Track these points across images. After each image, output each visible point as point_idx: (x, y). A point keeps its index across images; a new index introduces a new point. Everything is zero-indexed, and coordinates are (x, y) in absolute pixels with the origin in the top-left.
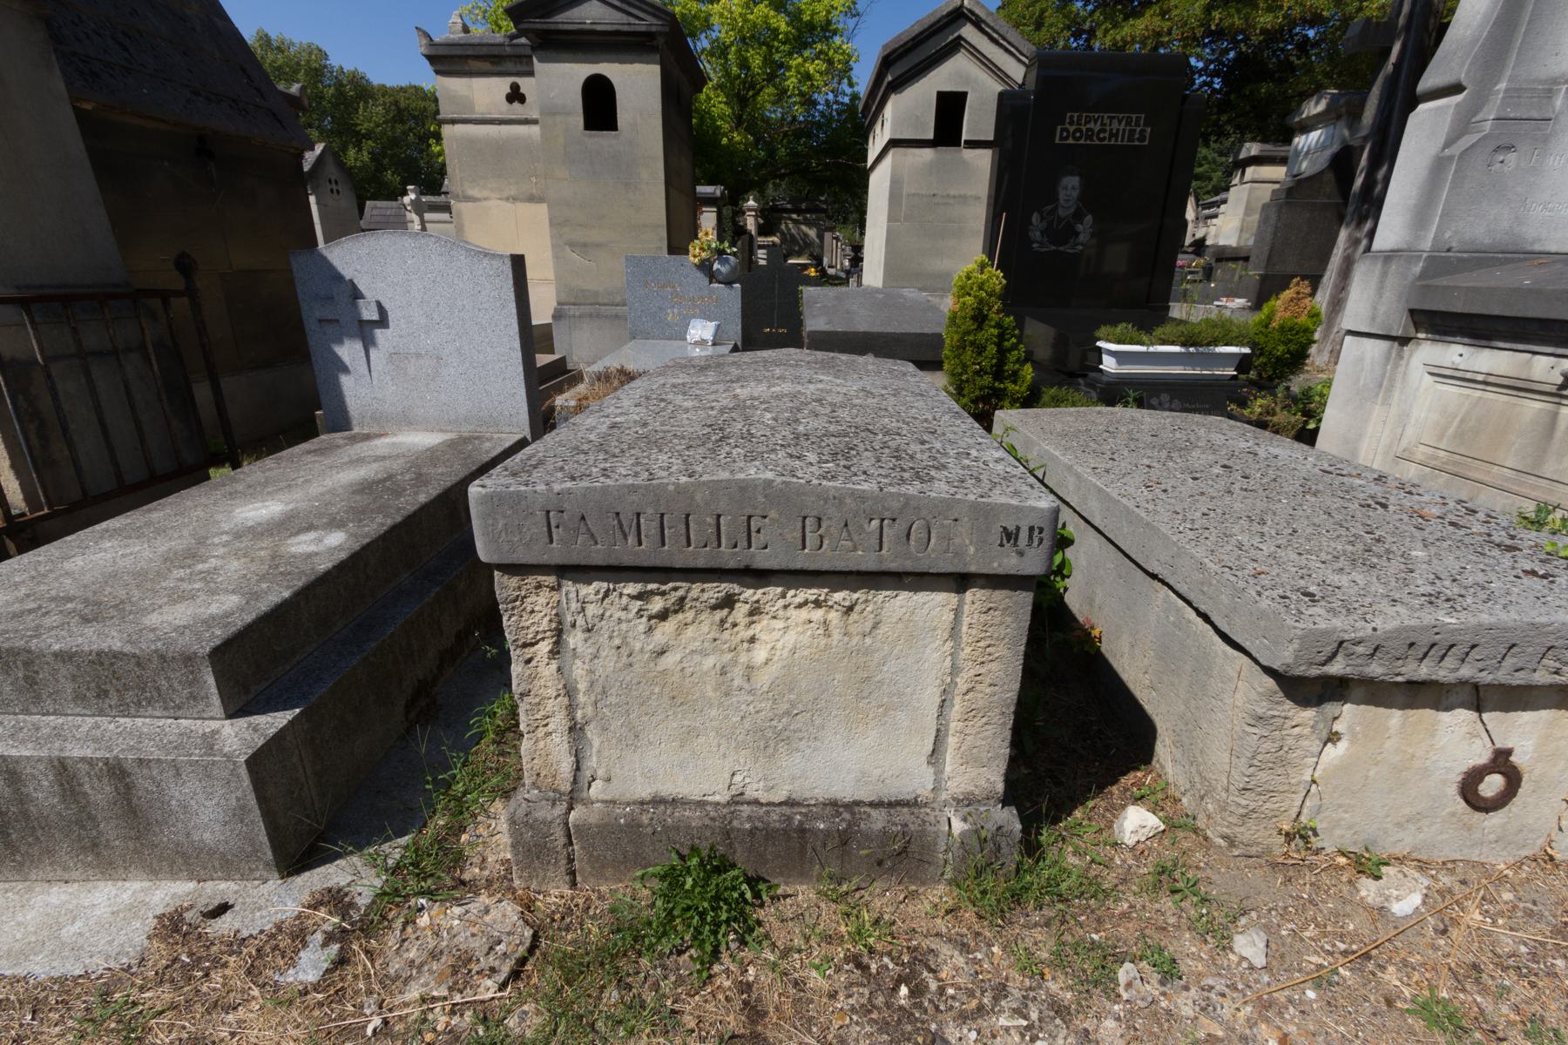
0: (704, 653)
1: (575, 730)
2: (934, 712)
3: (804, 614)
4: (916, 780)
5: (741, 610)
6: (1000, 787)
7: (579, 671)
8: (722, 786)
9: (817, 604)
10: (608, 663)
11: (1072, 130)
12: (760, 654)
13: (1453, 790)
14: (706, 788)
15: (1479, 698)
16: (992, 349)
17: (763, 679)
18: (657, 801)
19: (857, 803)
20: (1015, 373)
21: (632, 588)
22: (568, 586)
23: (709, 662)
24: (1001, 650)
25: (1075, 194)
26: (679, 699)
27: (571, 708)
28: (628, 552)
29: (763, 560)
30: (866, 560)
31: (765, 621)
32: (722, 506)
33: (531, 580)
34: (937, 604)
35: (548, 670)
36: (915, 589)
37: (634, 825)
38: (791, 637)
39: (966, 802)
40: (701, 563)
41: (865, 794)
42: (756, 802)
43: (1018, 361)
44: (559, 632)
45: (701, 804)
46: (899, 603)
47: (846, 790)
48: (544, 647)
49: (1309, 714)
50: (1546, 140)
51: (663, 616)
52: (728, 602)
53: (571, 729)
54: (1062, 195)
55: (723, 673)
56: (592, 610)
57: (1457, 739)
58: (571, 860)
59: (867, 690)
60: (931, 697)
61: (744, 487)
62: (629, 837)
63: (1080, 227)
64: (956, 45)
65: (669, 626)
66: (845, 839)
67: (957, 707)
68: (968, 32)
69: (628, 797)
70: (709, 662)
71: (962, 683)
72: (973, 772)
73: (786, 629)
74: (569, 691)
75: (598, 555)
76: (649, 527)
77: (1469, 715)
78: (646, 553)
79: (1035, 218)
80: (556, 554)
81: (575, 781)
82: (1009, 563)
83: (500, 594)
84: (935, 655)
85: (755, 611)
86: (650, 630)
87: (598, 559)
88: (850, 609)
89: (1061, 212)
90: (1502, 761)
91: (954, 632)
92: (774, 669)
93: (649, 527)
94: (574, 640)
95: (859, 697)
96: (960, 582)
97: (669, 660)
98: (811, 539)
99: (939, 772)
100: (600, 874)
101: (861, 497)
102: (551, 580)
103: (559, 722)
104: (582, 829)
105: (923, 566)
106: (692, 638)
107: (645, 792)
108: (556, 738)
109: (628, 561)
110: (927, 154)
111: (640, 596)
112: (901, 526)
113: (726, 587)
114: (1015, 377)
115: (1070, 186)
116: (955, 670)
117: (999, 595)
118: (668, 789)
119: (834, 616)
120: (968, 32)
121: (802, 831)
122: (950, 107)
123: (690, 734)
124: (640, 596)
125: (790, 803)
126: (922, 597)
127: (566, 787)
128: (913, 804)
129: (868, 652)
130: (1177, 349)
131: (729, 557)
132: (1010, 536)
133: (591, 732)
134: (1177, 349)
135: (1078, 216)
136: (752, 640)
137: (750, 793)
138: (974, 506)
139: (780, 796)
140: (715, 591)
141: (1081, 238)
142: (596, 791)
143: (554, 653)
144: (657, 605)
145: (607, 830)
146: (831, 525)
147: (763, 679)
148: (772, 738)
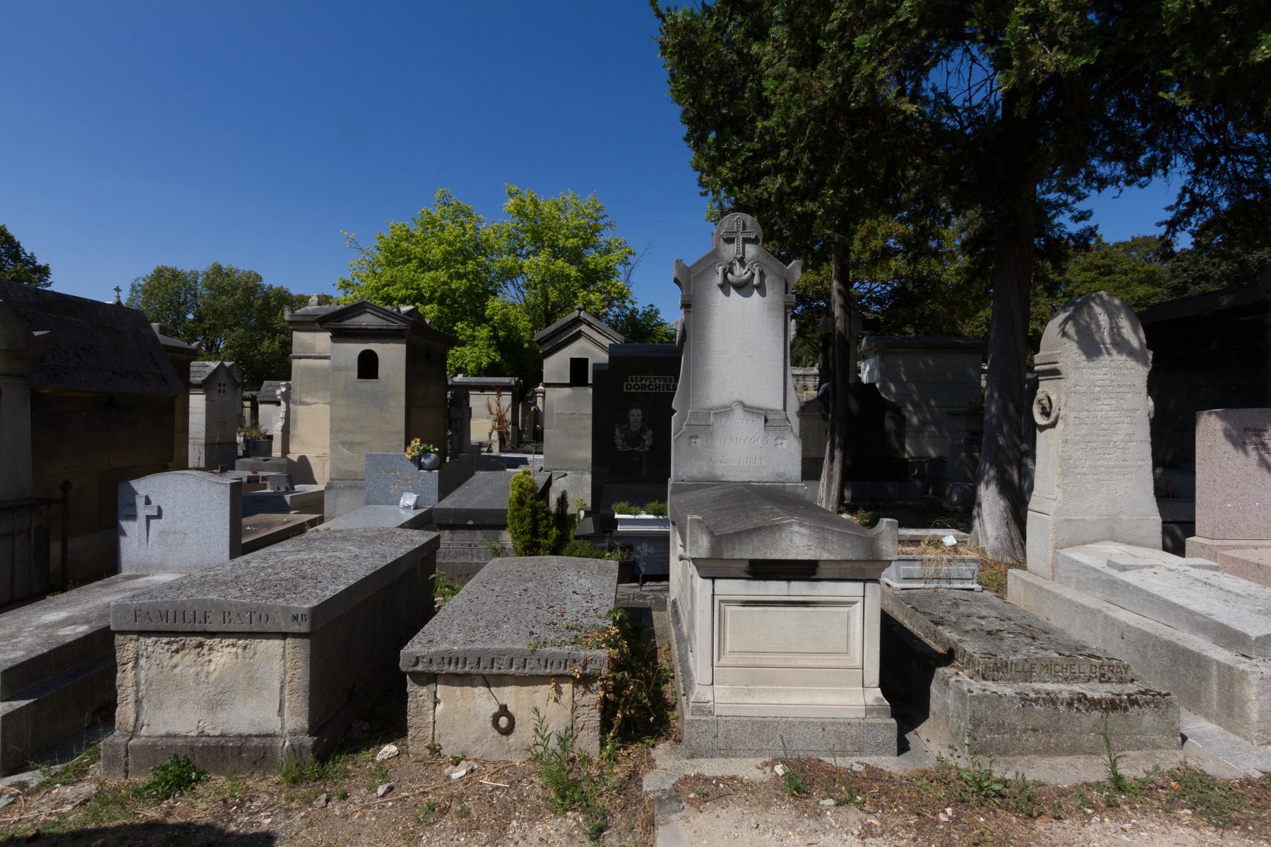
0: (190, 667)
1: (138, 702)
2: (278, 691)
3: (228, 650)
4: (274, 725)
5: (206, 648)
6: (307, 726)
7: (142, 675)
8: (194, 728)
9: (234, 645)
10: (154, 670)
11: (633, 384)
12: (212, 667)
13: (490, 725)
14: (188, 728)
15: (490, 681)
16: (528, 520)
17: (212, 677)
18: (168, 736)
19: (250, 736)
20: (546, 533)
21: (165, 640)
22: (142, 639)
23: (192, 670)
24: (300, 664)
25: (640, 418)
26: (179, 687)
27: (137, 691)
28: (163, 626)
29: (210, 628)
30: (246, 627)
31: (215, 653)
32: (196, 608)
33: (129, 637)
34: (276, 644)
35: (130, 675)
36: (268, 639)
37: (155, 745)
38: (224, 659)
39: (294, 733)
40: (188, 629)
41: (253, 731)
42: (209, 736)
43: (547, 525)
44: (137, 659)
45: (186, 737)
46: (263, 645)
47: (245, 729)
48: (131, 665)
49: (424, 690)
50: (711, 433)
51: (177, 651)
52: (201, 645)
53: (136, 701)
54: (632, 419)
55: (197, 674)
56: (150, 649)
57: (482, 701)
58: (127, 765)
59: (252, 682)
60: (277, 685)
61: (204, 601)
62: (152, 750)
63: (645, 437)
64: (579, 335)
65: (179, 656)
66: (240, 750)
67: (286, 691)
68: (584, 328)
69: (156, 734)
70: (192, 670)
71: (288, 680)
72: (295, 719)
73: (222, 656)
74: (137, 684)
75: (152, 627)
76: (171, 616)
77: (484, 689)
78: (169, 626)
79: (617, 432)
80: (137, 627)
81: (135, 727)
82: (296, 628)
83: (116, 643)
84: (277, 666)
85: (211, 649)
86: (171, 657)
87: (152, 628)
88: (245, 647)
89: (633, 429)
90: (504, 710)
91: (284, 657)
92: (216, 674)
93: (171, 616)
94: (142, 662)
95: (249, 685)
96: (284, 636)
97: (177, 670)
98: (227, 620)
99: (283, 720)
100: (138, 774)
101: (243, 604)
102: (135, 637)
103: (131, 698)
104: (133, 747)
105: (266, 630)
106: (187, 662)
107: (163, 732)
108: (130, 706)
109: (162, 629)
110: (567, 391)
111: (167, 643)
112: (258, 614)
113: (202, 639)
114: (546, 536)
115: (636, 414)
116: (285, 673)
117: (298, 640)
118: (173, 729)
119: (240, 651)
120: (584, 328)
121: (223, 747)
122: (578, 366)
123: (183, 702)
124: (167, 643)
125: (222, 736)
126: (271, 642)
127: (131, 729)
128: (273, 736)
129: (252, 665)
130: (652, 517)
131: (198, 627)
132: (295, 618)
133: (145, 704)
134: (652, 517)
135: (643, 431)
136: (210, 661)
137: (207, 732)
138: (283, 607)
139: (217, 733)
140: (195, 640)
141: (647, 443)
142: (144, 731)
143: (134, 667)
144: (175, 647)
145: (143, 747)
146: (234, 616)
147: (212, 677)
148: (214, 705)
